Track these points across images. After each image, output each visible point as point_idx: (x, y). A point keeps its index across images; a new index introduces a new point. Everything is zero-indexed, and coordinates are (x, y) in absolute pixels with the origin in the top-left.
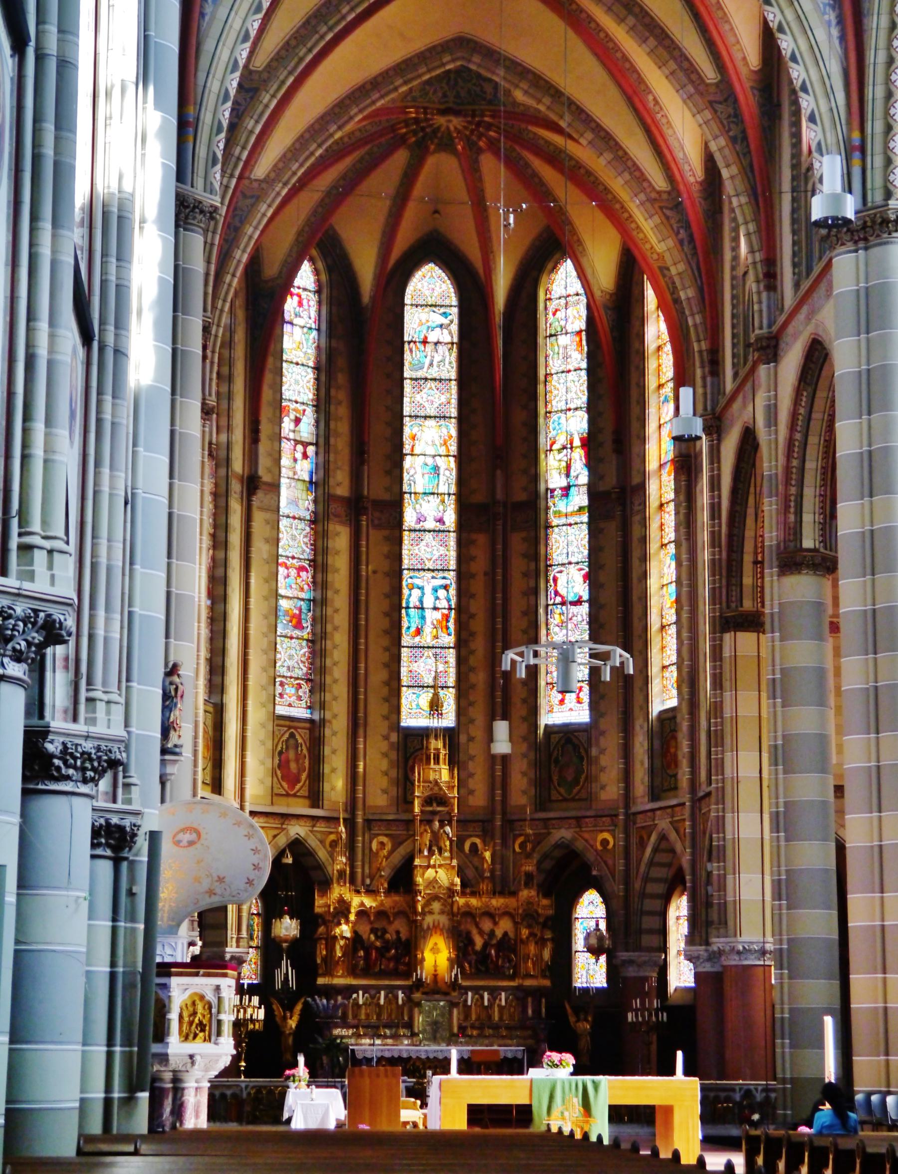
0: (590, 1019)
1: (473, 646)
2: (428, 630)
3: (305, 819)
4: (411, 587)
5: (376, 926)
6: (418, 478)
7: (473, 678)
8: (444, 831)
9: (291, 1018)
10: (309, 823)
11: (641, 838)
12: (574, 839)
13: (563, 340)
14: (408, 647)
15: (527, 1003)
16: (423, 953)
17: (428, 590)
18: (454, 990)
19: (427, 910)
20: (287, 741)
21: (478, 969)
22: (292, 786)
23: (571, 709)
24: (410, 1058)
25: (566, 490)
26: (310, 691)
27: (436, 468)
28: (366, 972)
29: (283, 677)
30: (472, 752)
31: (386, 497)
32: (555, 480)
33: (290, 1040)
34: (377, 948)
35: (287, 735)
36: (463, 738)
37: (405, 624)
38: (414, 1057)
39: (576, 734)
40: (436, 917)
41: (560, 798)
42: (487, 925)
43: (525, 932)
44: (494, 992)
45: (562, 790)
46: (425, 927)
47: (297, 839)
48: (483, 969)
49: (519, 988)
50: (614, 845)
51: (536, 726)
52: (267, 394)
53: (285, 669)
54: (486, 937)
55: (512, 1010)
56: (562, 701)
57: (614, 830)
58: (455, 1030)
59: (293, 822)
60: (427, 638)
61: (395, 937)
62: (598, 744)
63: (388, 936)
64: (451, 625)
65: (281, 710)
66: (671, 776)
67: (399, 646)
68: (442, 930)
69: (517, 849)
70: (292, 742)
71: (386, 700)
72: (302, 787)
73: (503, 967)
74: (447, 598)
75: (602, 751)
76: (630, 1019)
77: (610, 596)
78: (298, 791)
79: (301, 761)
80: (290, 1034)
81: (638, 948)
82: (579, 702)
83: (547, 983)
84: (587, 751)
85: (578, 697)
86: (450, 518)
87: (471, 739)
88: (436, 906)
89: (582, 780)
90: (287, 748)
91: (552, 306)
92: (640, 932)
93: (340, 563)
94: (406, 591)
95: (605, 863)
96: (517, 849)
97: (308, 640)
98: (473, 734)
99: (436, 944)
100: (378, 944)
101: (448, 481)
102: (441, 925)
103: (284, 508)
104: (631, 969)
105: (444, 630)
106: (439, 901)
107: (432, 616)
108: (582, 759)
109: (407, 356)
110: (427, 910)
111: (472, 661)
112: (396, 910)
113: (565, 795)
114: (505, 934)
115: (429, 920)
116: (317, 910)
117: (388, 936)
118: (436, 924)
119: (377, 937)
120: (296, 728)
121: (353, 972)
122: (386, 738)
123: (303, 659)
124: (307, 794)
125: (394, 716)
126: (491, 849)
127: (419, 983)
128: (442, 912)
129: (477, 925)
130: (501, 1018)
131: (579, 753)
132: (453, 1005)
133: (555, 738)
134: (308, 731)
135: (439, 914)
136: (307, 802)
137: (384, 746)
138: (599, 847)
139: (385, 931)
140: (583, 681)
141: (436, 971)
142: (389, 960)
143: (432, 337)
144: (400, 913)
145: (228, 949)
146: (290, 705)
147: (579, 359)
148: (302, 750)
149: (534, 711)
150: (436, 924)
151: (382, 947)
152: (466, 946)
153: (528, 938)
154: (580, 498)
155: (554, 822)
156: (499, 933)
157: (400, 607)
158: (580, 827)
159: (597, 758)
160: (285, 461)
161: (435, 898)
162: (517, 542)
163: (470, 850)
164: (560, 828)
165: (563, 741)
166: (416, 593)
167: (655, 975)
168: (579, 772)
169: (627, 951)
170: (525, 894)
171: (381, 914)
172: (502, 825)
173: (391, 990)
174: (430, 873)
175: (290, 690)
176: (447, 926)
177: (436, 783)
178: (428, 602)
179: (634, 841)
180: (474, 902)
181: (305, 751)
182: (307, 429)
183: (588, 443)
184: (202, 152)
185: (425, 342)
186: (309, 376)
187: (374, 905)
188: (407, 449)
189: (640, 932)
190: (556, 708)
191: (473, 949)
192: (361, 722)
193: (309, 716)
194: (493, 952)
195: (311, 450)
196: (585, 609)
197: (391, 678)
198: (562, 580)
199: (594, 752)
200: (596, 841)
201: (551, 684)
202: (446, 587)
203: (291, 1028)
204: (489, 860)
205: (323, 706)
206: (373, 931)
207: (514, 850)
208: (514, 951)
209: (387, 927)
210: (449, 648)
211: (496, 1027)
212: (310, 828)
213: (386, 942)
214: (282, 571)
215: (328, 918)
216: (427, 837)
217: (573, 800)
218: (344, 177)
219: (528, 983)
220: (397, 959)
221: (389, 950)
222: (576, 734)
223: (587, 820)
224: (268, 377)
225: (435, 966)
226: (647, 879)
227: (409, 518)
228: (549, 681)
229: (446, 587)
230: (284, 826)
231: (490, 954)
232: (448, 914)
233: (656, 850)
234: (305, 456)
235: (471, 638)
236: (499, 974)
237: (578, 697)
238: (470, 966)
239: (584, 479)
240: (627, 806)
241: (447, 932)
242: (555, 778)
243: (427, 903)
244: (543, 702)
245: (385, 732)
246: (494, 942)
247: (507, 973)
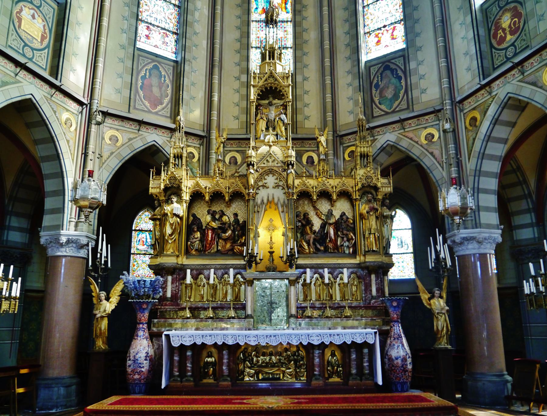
0: (444, 295)
1: (304, 14)
3: (163, 131)
5: (213, 209)
7: (305, 36)
8: (280, 118)
9: (108, 299)
10: (167, 134)
11: (474, 119)
12: (399, 139)
14: (256, 21)
15: (370, 280)
16: (257, 228)
18: (291, 266)
19: (260, 184)
20: (150, 70)
21: (317, 250)
22: (156, 106)
23: (387, 46)
24: (237, 345)
26: (176, 41)
28: (202, 252)
29: (151, 24)
30: (306, 88)
33: (104, 324)
34: (213, 229)
35: (151, 66)
36: (299, 78)
38: (242, 343)
39: (393, 61)
40: (271, 191)
41: (383, 113)
42: (324, 206)
43: (364, 208)
44: (334, 269)
45: (383, 107)
46: (259, 202)
47: (154, 145)
48: (322, 248)
49: (359, 266)
50: (439, 137)
51: (358, 61)
53: (153, 19)
54: (323, 217)
55: (354, 288)
56: (379, 41)
57: (439, 124)
58: (293, 311)
59: (151, 130)
61: (232, 219)
62: (416, 59)
63: (225, 218)
66: (506, 49)
68: (277, 204)
69: (347, 158)
70: (155, 72)
71: (238, 52)
72: (163, 109)
73: (342, 245)
75: (420, 63)
76: (527, 291)
78: (160, 111)
79: (163, 88)
80: (102, 317)
81: (477, 225)
82: (393, 39)
84: (405, 72)
85: (392, 35)
87: (305, 79)
88: (270, 180)
89: (401, 95)
90: (150, 74)
95: (432, 154)
96: (347, 158)
97: (175, 5)
98: (306, 75)
99: (271, 220)
100: (214, 225)
102: (276, 200)
104: (470, 246)
105: (284, 10)
106: (274, 175)
108: (400, 78)
110: (260, 184)
111: (305, 24)
112: (231, 190)
113: (386, 110)
114: (343, 214)
115: (263, 194)
116: (151, 191)
117: (225, 218)
118: (270, 199)
119: (214, 219)
120: (159, 63)
121: (188, 253)
122: (238, 79)
123: (170, 17)
124: (169, 115)
125: (244, 64)
126: (325, 135)
127: (252, 259)
128: (277, 186)
129: (315, 208)
130: (343, 298)
131: (397, 74)
132: (292, 283)
133: (373, 70)
134: (172, 68)
135: (273, 188)
136: (169, 120)
137: (237, 85)
138: (425, 142)
139: (223, 214)
140: (396, 23)
141: (271, 248)
142: (226, 240)
144: (237, 196)
145: (62, 232)
146: (156, 46)
148: (165, 81)
149: (356, 50)
150: (270, 199)
151: (219, 228)
152: (304, 226)
153: (368, 212)
155: (378, 129)
156: (337, 214)
158: (404, 129)
159: (416, 69)
161: (271, 171)
163: (307, 162)
164: (385, 134)
165: (382, 69)
167: (493, 252)
169: (466, 228)
170: (361, 172)
171: (217, 196)
172: (333, 140)
173: (226, 268)
174: (264, 149)
176: (282, 201)
177: (272, 75)
180: (312, 182)
181: (167, 81)
187: (209, 185)
190: (373, 49)
191: (311, 229)
192: (217, 63)
193: (175, 59)
194: (332, 232)
197: (241, 37)
200: (420, 137)
201: (368, 33)
203: (105, 311)
204: (324, 144)
205: (184, 48)
206: (213, 214)
207: (344, 159)
208: (354, 230)
209: (225, 210)
210: (287, 21)
211: (340, 308)
212: (169, 139)
213: (224, 224)
215: (162, 198)
216: (262, 125)
217: (394, 112)
219: (370, 259)
220: (233, 240)
221: (225, 232)
222: (393, 61)
223: (410, 122)
225: (271, 243)
226: (482, 156)
228: (366, 31)
230: (140, 132)
231: (328, 233)
232: (283, 189)
233: (496, 122)
235: (304, 9)
236: (337, 251)
237: (392, 35)
238: (309, 245)
240: (452, 97)
241: (282, 206)
242: (376, 100)
243: (261, 177)
244: (363, 45)
245: (237, 75)
246: (332, 221)
247: (347, 252)
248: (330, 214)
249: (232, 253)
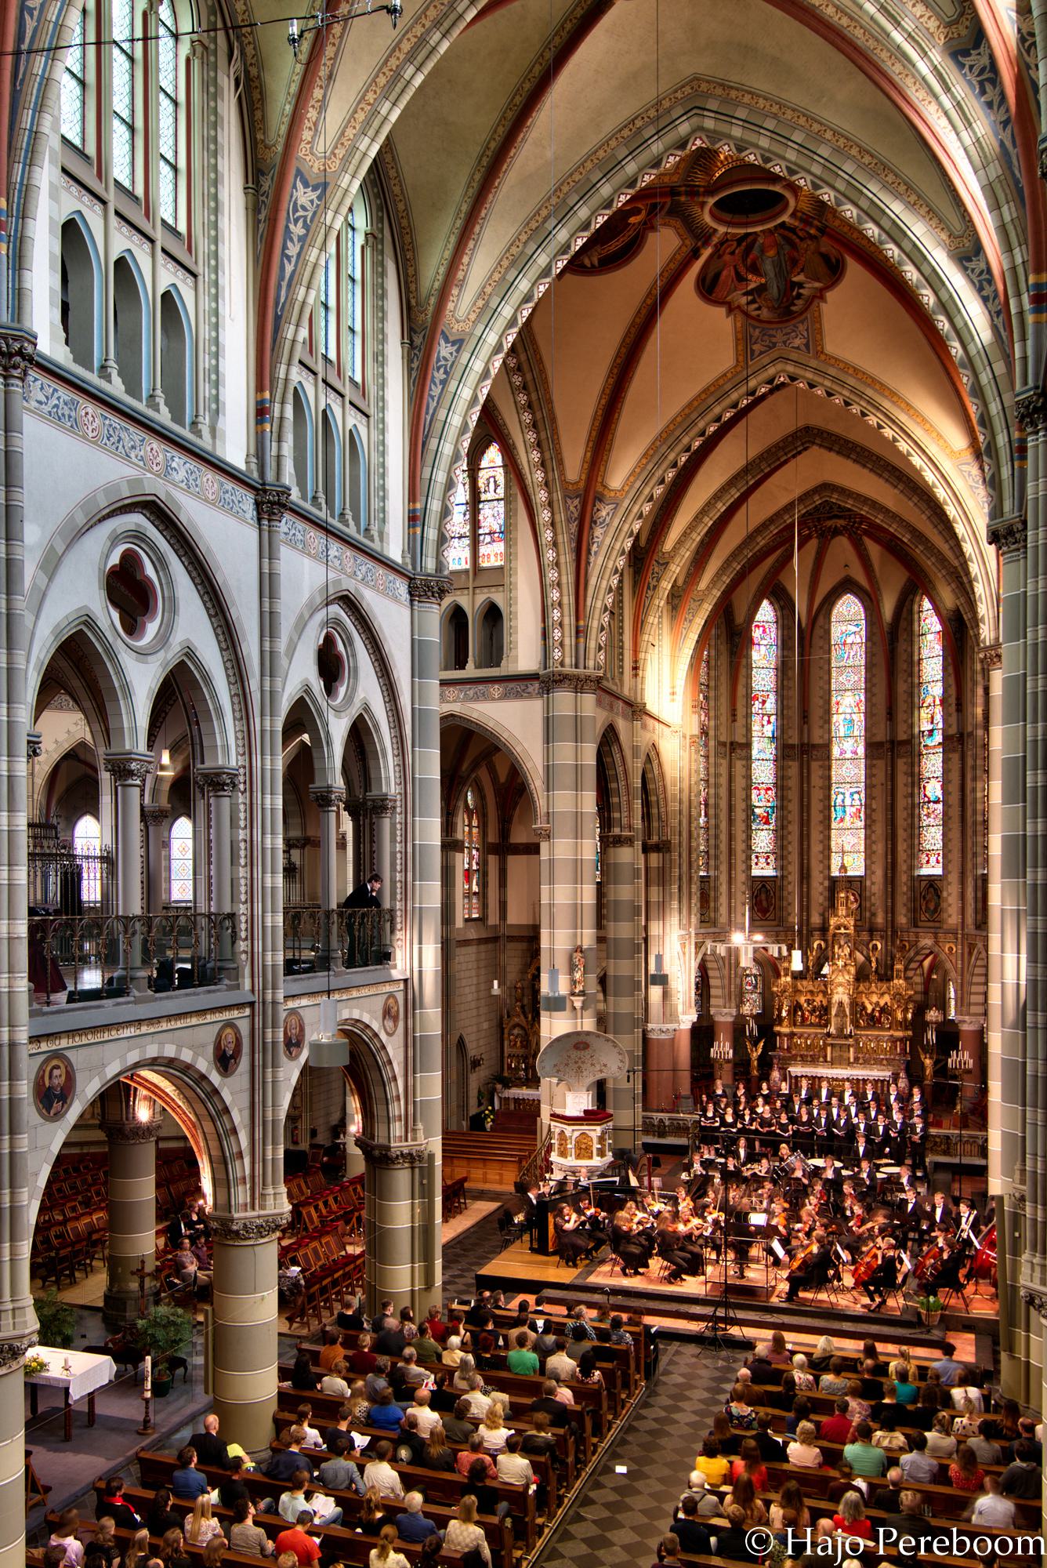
2: (847, 818)
4: (837, 794)
6: (841, 728)
13: (930, 637)
17: (847, 795)
25: (931, 732)
27: (852, 721)
31: (821, 742)
32: (926, 726)
37: (833, 816)
52: (741, 691)
60: (847, 823)
64: (862, 815)
65: (756, 872)
67: (829, 828)
74: (859, 799)
77: (955, 799)
83: (910, 1033)
86: (861, 751)
88: (840, 989)
91: (923, 616)
92: (970, 1004)
93: (793, 783)
94: (833, 796)
101: (859, 729)
103: (755, 753)
107: (850, 810)
109: (833, 653)
137: (821, 889)
143: (849, 641)
147: (938, 649)
154: (938, 738)
156: (882, 1003)
157: (829, 806)
160: (756, 727)
162: (901, 765)
166: (840, 797)
168: (937, 906)
175: (762, 860)
178: (848, 802)
179: (966, 950)
182: (771, 706)
183: (942, 702)
184: (592, 645)
185: (844, 644)
186: (772, 673)
188: (834, 710)
189: (970, 1004)
195: (773, 719)
196: (940, 806)
198: (929, 787)
199: (945, 894)
202: (858, 793)
214: (754, 792)
218: (777, 561)
224: (742, 681)
227: (836, 752)
229: (858, 793)
234: (769, 722)
239: (940, 726)
248: (877, 1004)
249: (819, 1025)
